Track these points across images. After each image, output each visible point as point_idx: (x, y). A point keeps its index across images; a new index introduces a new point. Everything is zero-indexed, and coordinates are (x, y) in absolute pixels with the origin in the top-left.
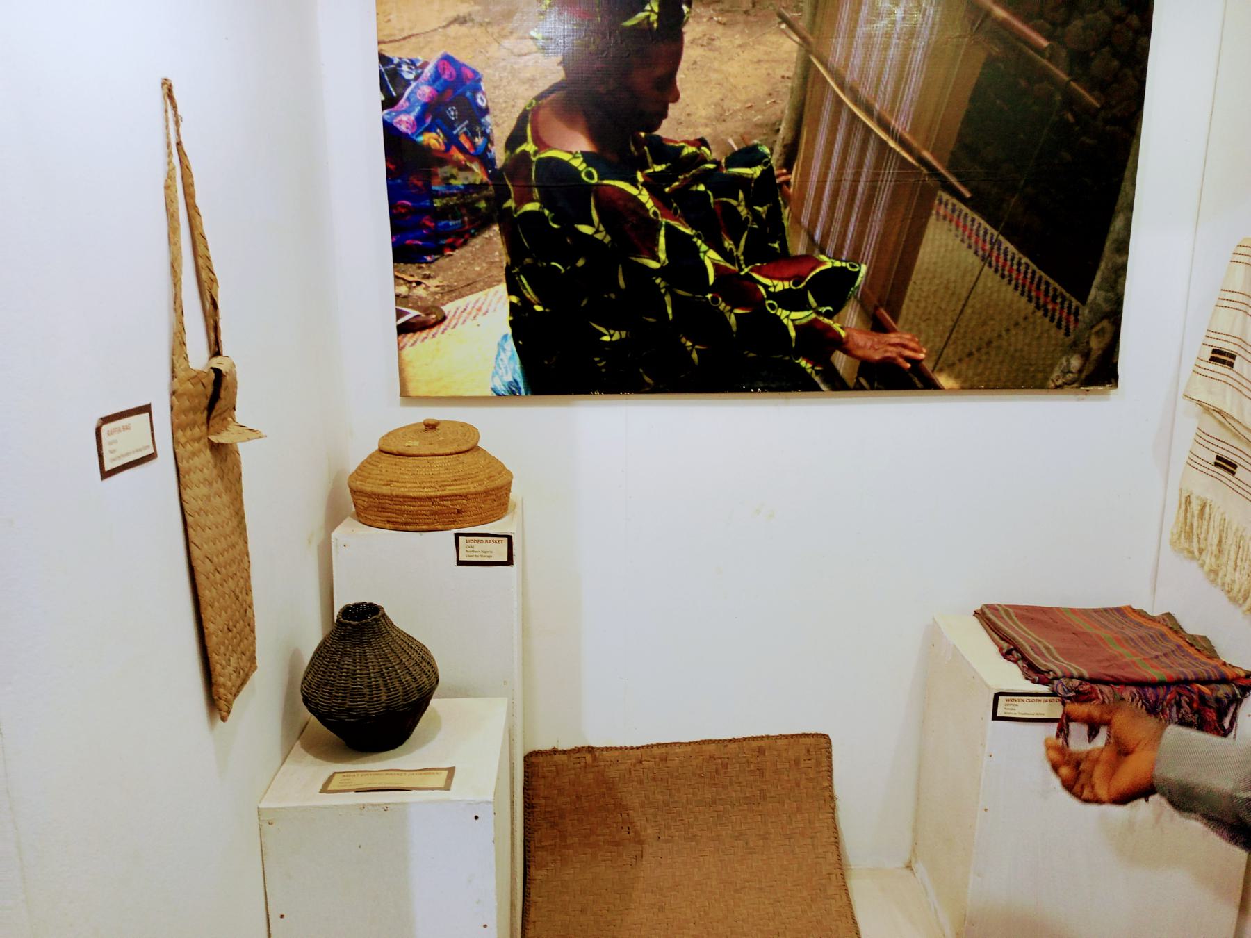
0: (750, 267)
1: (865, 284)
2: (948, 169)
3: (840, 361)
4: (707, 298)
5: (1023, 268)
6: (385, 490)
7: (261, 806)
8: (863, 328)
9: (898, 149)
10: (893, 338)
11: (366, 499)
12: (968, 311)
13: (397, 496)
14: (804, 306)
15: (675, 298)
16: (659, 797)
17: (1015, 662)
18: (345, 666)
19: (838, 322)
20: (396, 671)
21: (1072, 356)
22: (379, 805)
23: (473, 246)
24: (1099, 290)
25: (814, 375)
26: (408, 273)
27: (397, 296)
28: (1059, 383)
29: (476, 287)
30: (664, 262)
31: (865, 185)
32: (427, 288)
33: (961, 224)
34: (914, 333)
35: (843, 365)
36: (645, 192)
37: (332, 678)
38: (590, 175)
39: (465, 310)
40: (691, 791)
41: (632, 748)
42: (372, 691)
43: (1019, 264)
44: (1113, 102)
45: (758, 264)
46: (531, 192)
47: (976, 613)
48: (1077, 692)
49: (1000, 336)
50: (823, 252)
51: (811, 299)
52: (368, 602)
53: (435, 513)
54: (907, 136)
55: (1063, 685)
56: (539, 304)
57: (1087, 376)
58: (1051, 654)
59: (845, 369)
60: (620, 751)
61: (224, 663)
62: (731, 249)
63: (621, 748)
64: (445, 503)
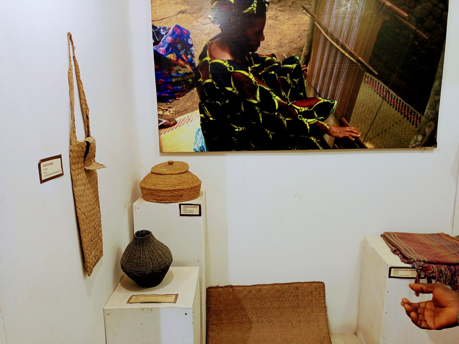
0: (292, 102)
1: (336, 108)
2: (369, 64)
3: (327, 138)
4: (275, 114)
5: (398, 102)
6: (153, 187)
7: (105, 308)
8: (336, 125)
9: (349, 57)
10: (348, 129)
11: (146, 191)
12: (377, 118)
13: (157, 190)
14: (312, 117)
15: (263, 115)
16: (258, 305)
17: (398, 255)
18: (137, 254)
19: (326, 123)
20: (156, 256)
21: (419, 135)
23: (187, 96)
24: (429, 110)
25: (317, 143)
26: (163, 106)
27: (159, 115)
28: (414, 145)
29: (188, 111)
30: (259, 101)
31: (336, 71)
32: (170, 112)
33: (374, 85)
34: (356, 127)
35: (328, 139)
36: (251, 74)
37: (132, 259)
38: (231, 69)
39: (184, 120)
40: (270, 303)
41: (247, 286)
43: (397, 100)
44: (434, 37)
45: (295, 101)
46: (208, 75)
47: (381, 236)
48: (423, 267)
49: (390, 128)
50: (320, 96)
51: (315, 114)
53: (172, 196)
54: (353, 52)
55: (417, 264)
56: (211, 117)
57: (424, 143)
58: (412, 252)
59: (329, 141)
61: (89, 253)
62: (284, 96)
63: (243, 286)
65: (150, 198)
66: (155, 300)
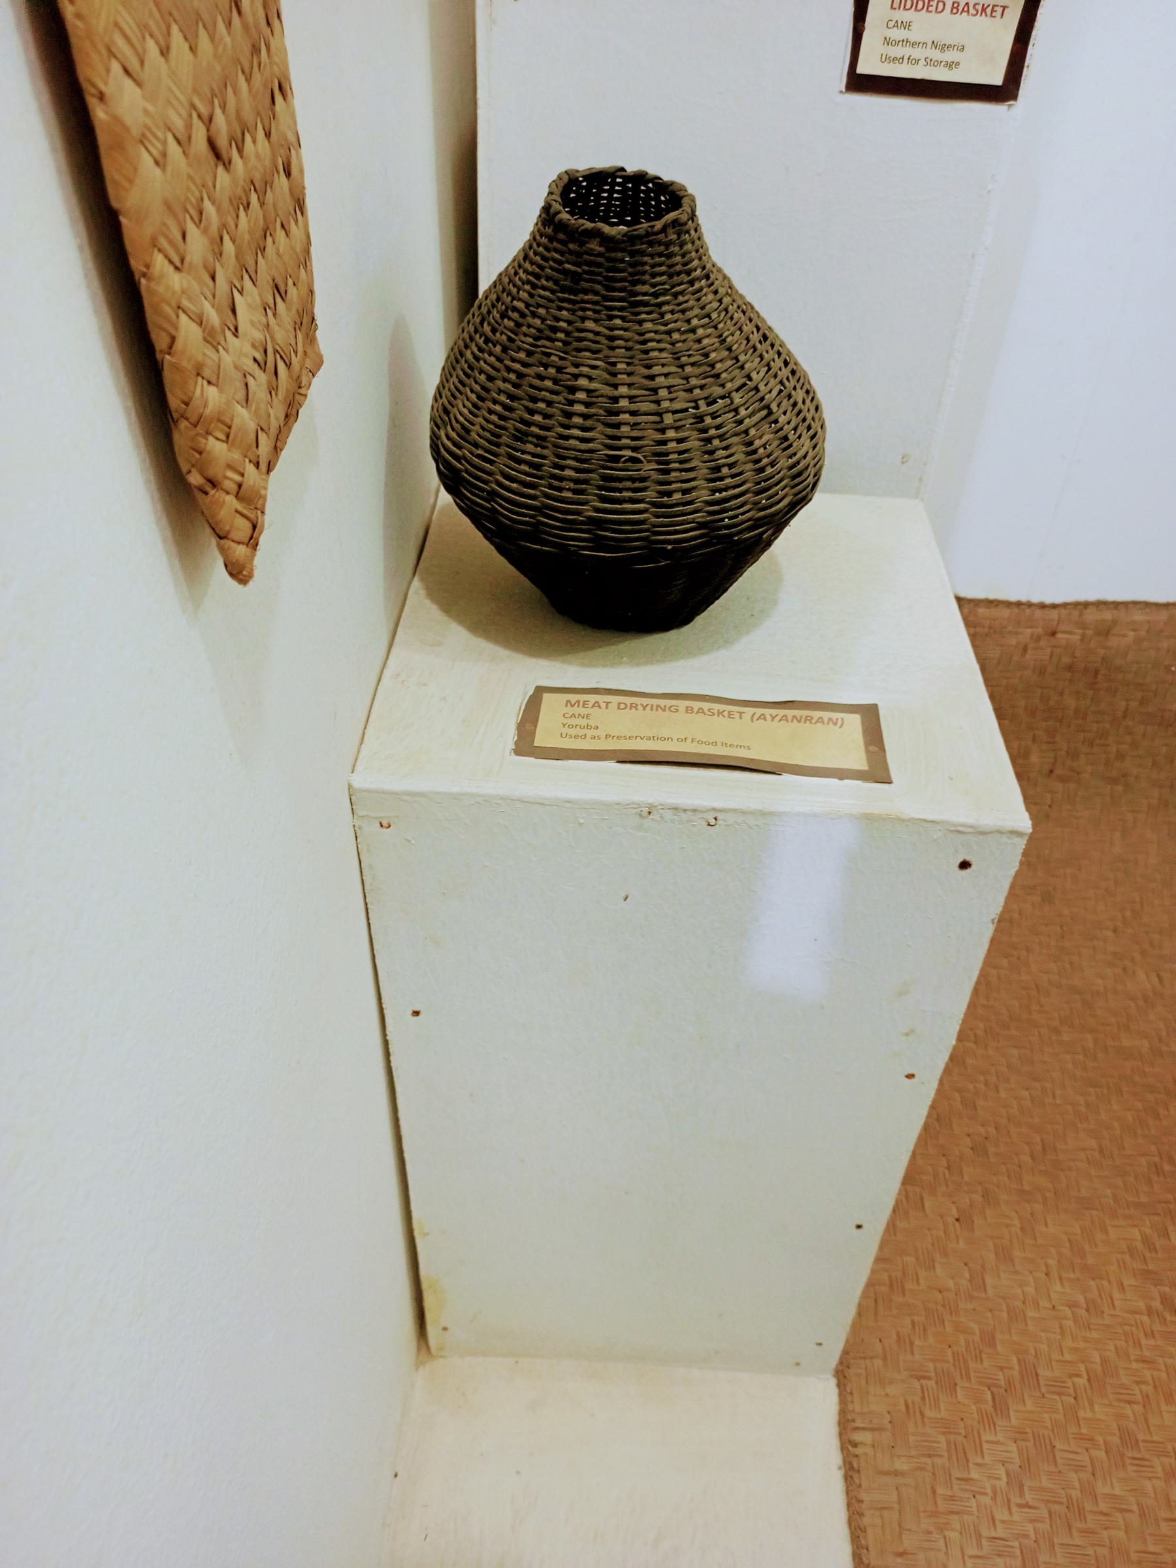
7: (358, 781)
16: (1070, 702)
18: (583, 382)
20: (736, 410)
22: (694, 811)
41: (1042, 606)
42: (667, 472)
52: (631, 168)
60: (1016, 610)
61: (213, 316)
63: (1019, 604)
66: (724, 744)
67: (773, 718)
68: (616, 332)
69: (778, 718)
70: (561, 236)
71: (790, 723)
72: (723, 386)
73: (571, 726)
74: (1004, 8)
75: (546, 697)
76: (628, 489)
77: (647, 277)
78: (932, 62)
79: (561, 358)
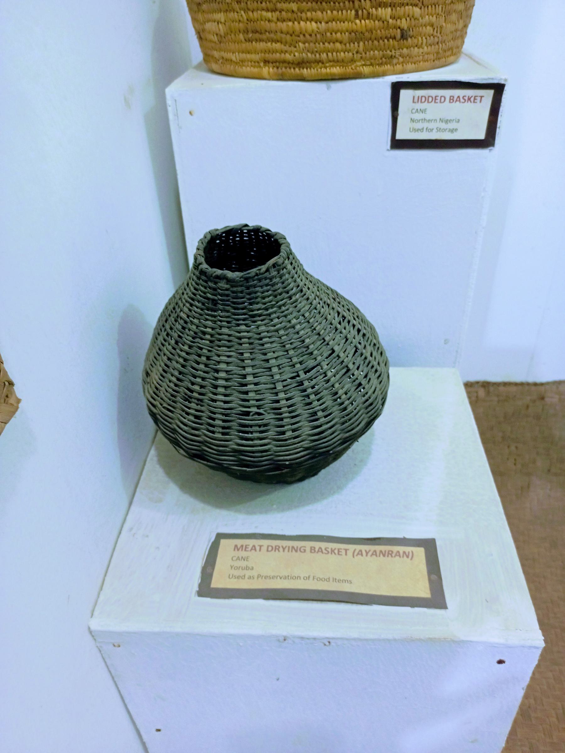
7: (95, 625)
18: (223, 366)
42: (282, 419)
63: (522, 384)
64: (381, 12)
65: (244, 56)
67: (367, 553)
68: (242, 334)
69: (370, 553)
70: (203, 278)
71: (378, 558)
72: (315, 359)
73: (238, 568)
74: (481, 97)
75: (223, 542)
76: (256, 432)
77: (259, 299)
78: (441, 130)
79: (209, 351)
